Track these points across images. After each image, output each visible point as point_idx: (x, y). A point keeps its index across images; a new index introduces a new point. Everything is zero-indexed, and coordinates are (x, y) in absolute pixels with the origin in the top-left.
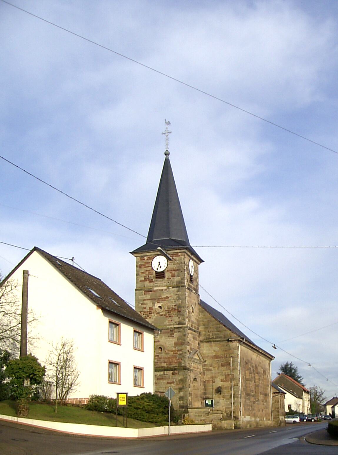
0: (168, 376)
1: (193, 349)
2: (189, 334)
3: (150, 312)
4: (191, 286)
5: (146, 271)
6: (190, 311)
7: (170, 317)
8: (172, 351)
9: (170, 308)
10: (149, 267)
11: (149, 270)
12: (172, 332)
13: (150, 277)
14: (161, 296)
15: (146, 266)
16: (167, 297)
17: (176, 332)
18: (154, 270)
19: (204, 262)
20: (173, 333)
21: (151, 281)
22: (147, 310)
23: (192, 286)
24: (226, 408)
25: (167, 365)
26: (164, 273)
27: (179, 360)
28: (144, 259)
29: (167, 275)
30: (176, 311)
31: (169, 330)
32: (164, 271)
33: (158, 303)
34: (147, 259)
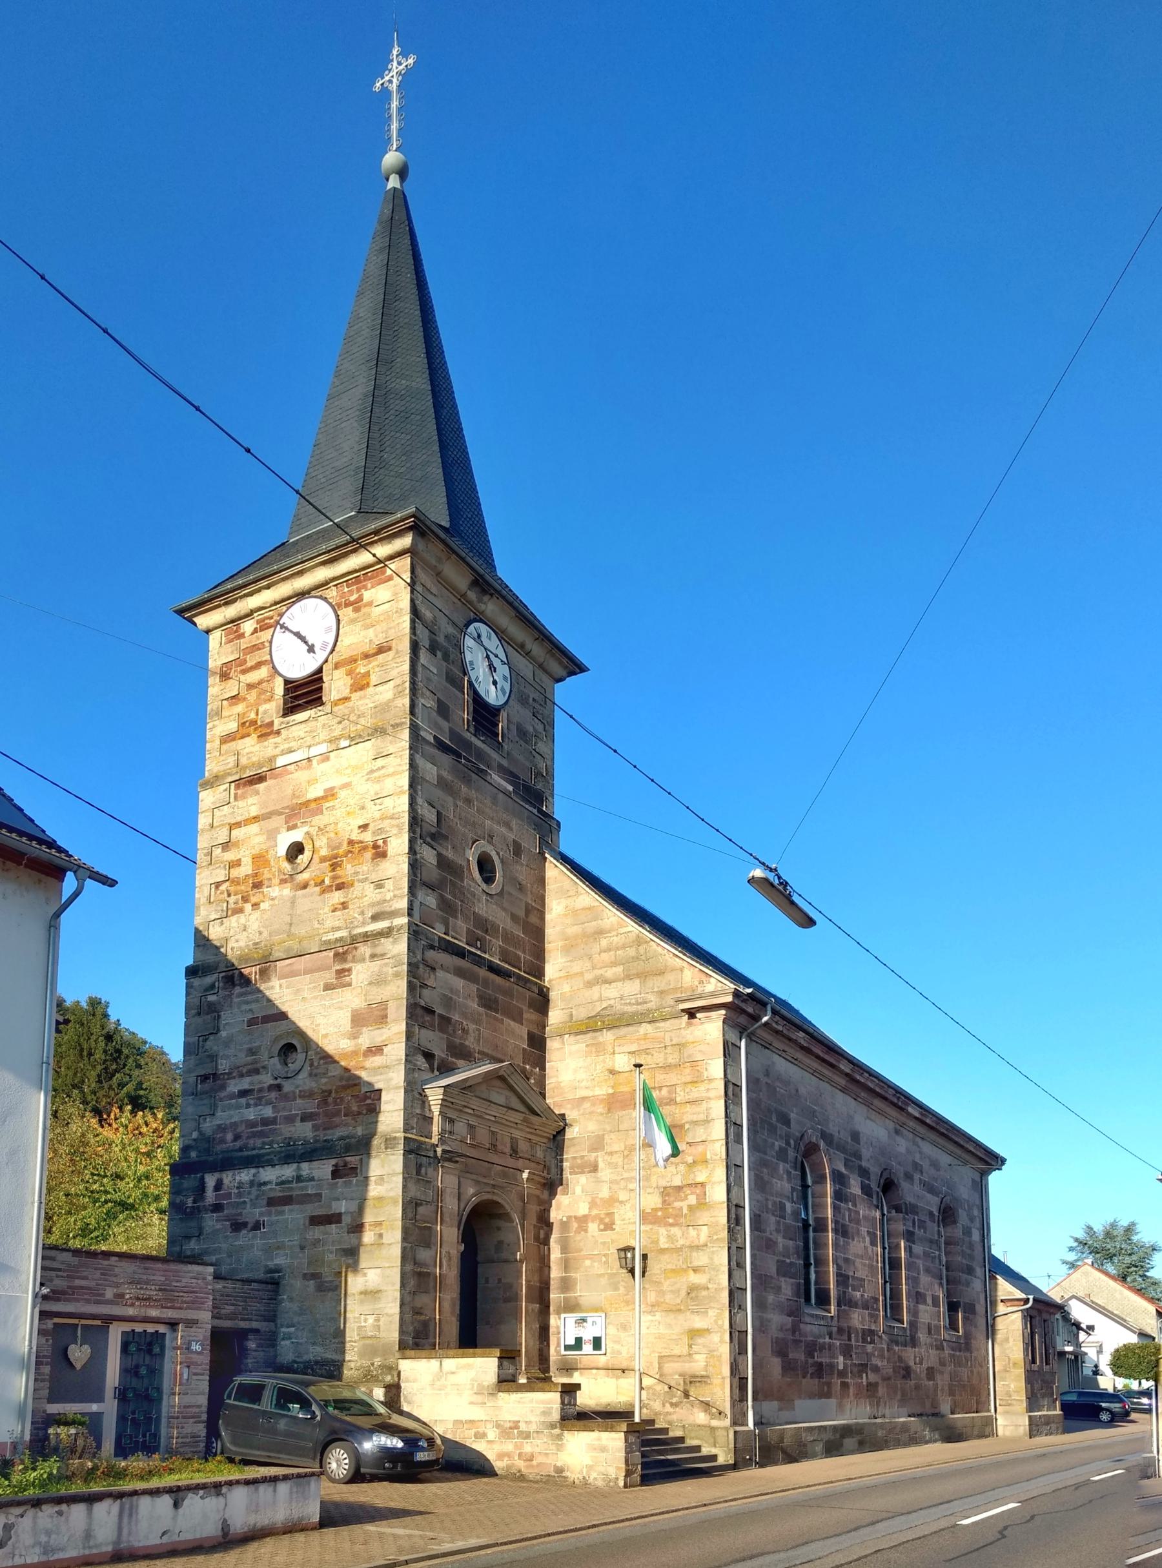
0: (313, 1187)
5: (250, 687)
9: (338, 847)
10: (259, 665)
11: (260, 683)
12: (345, 960)
13: (265, 712)
15: (249, 664)
17: (363, 960)
18: (280, 675)
20: (347, 966)
21: (267, 731)
22: (246, 869)
25: (315, 1128)
26: (321, 679)
28: (242, 636)
29: (335, 685)
30: (369, 854)
31: (331, 954)
32: (320, 670)
33: (289, 829)
34: (255, 631)
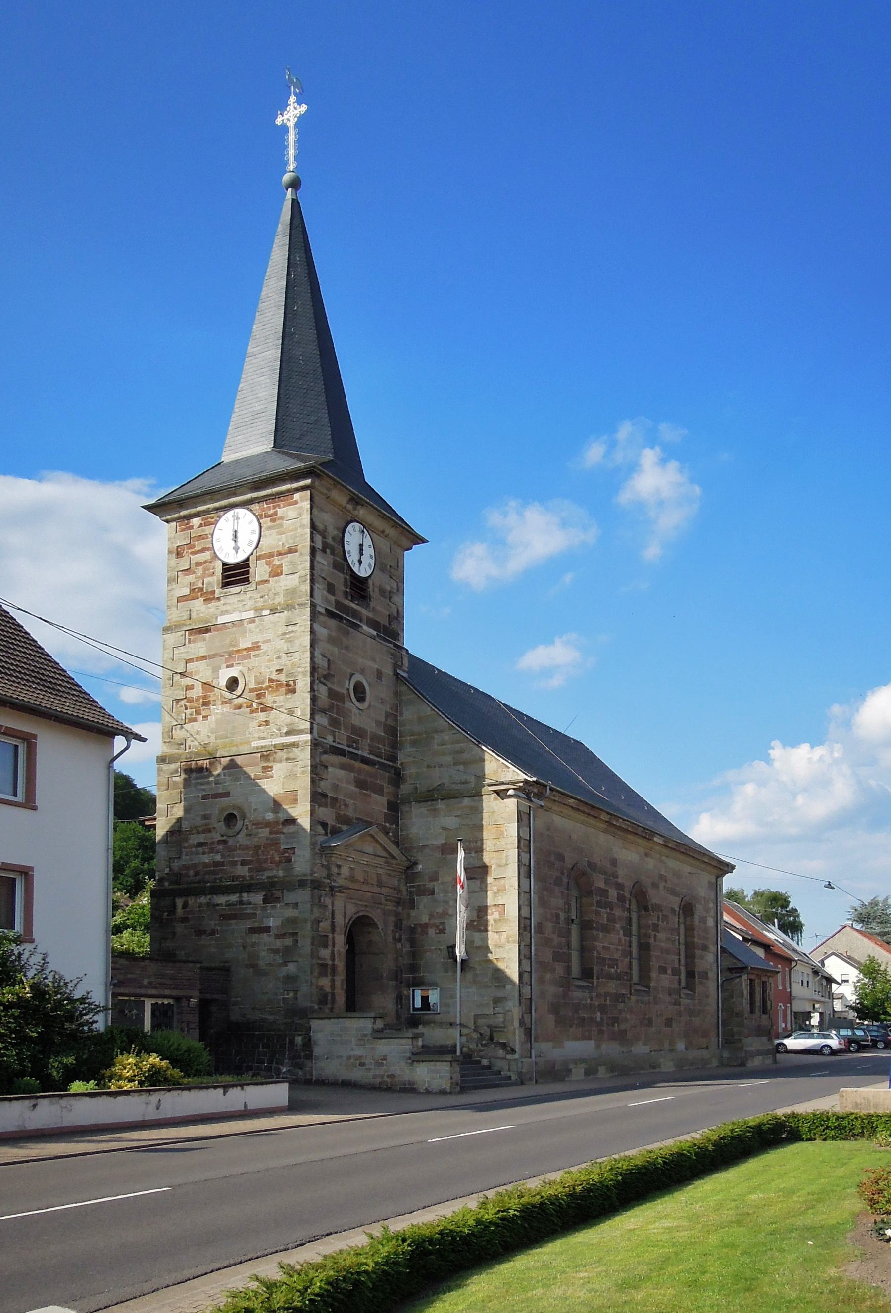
0: (251, 908)
1: (358, 819)
2: (330, 769)
3: (205, 697)
4: (360, 613)
5: (198, 564)
6: (345, 692)
7: (263, 711)
8: (268, 824)
9: (263, 683)
10: (203, 550)
11: (205, 562)
12: (268, 761)
13: (209, 583)
14: (238, 645)
15: (197, 548)
16: (256, 647)
17: (281, 761)
18: (219, 559)
19: (424, 541)
20: (270, 765)
21: (210, 597)
22: (197, 692)
23: (364, 612)
24: (476, 1017)
25: (250, 870)
26: (248, 566)
27: (287, 855)
28: (191, 528)
29: (259, 571)
30: (283, 689)
31: (259, 755)
32: (248, 559)
33: (228, 667)
34: (201, 526)
